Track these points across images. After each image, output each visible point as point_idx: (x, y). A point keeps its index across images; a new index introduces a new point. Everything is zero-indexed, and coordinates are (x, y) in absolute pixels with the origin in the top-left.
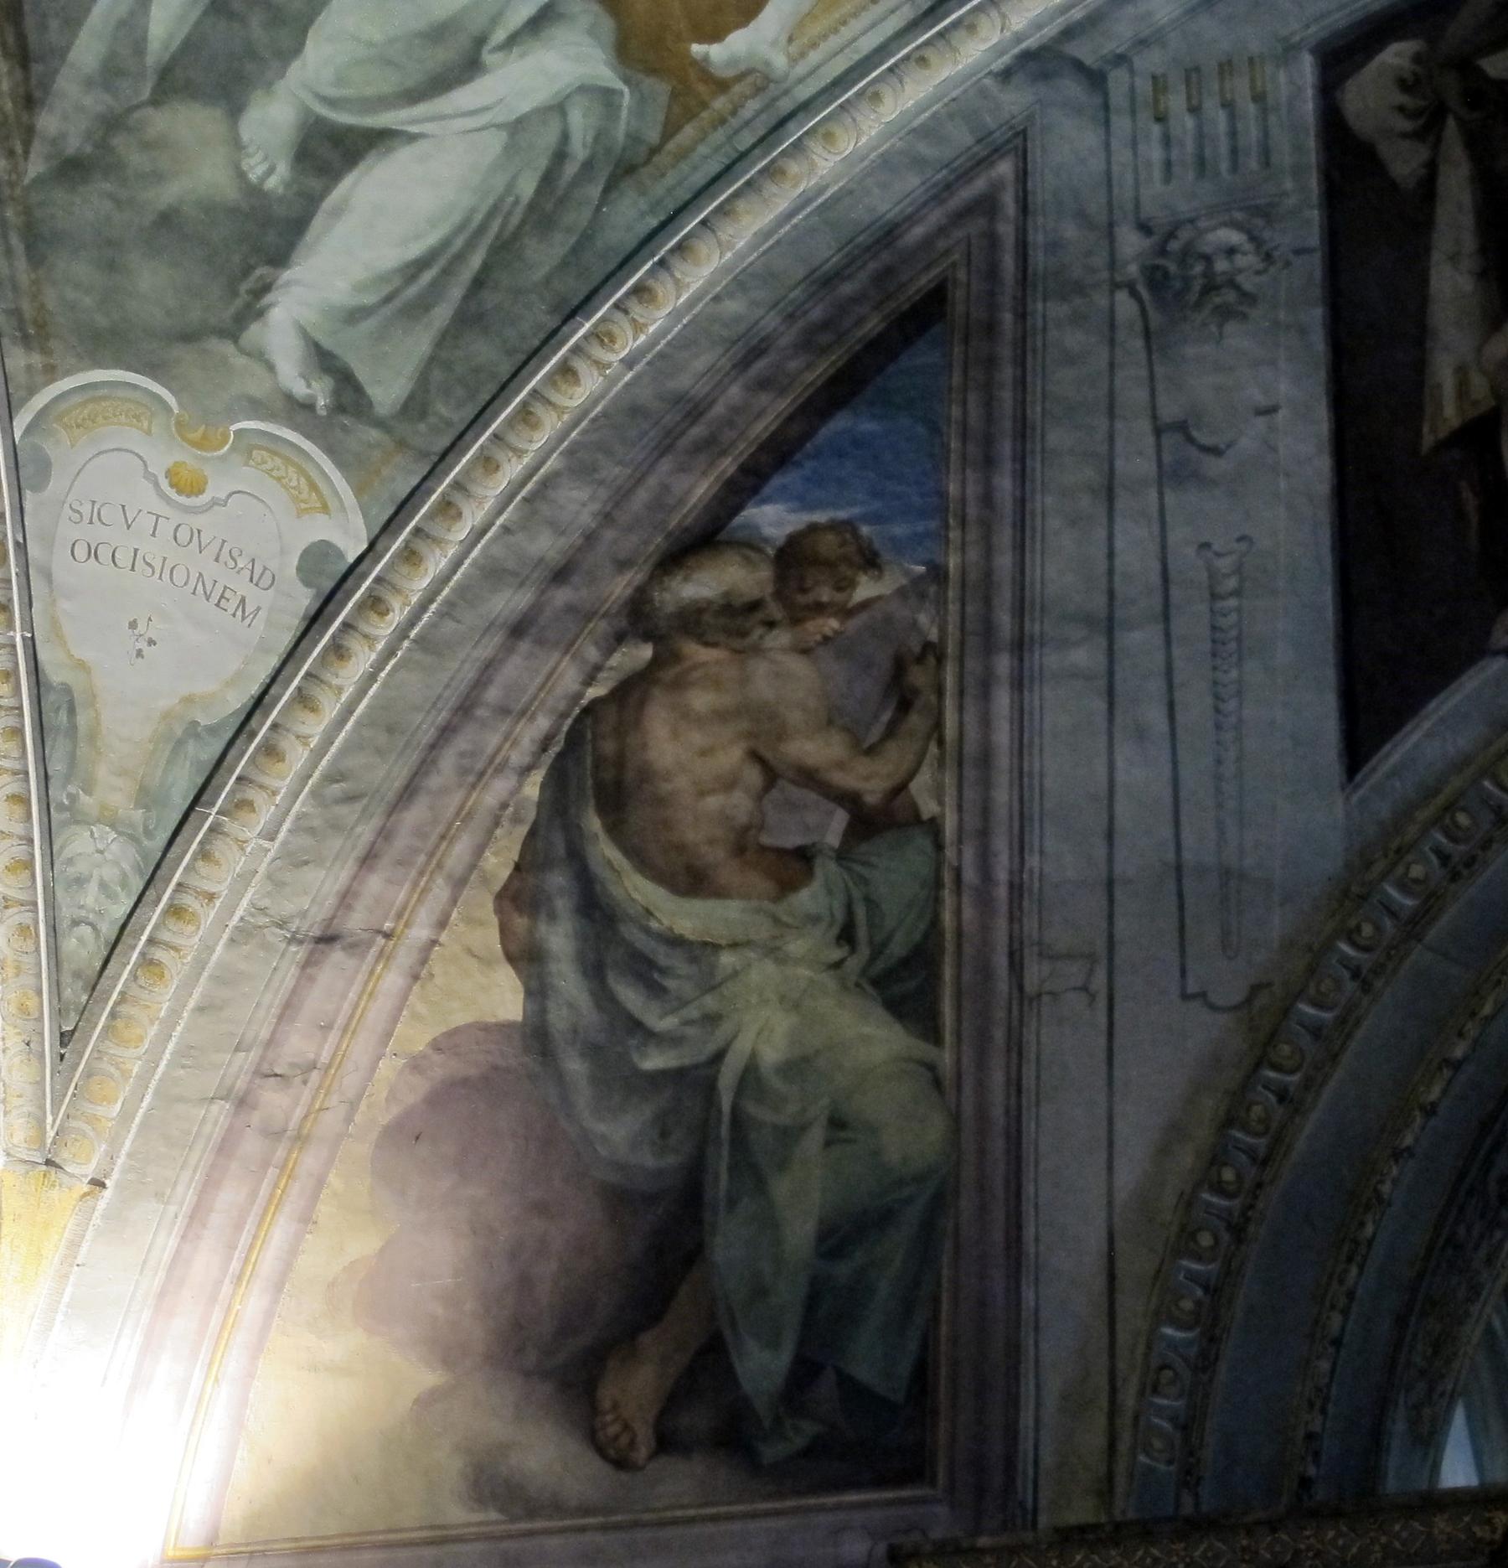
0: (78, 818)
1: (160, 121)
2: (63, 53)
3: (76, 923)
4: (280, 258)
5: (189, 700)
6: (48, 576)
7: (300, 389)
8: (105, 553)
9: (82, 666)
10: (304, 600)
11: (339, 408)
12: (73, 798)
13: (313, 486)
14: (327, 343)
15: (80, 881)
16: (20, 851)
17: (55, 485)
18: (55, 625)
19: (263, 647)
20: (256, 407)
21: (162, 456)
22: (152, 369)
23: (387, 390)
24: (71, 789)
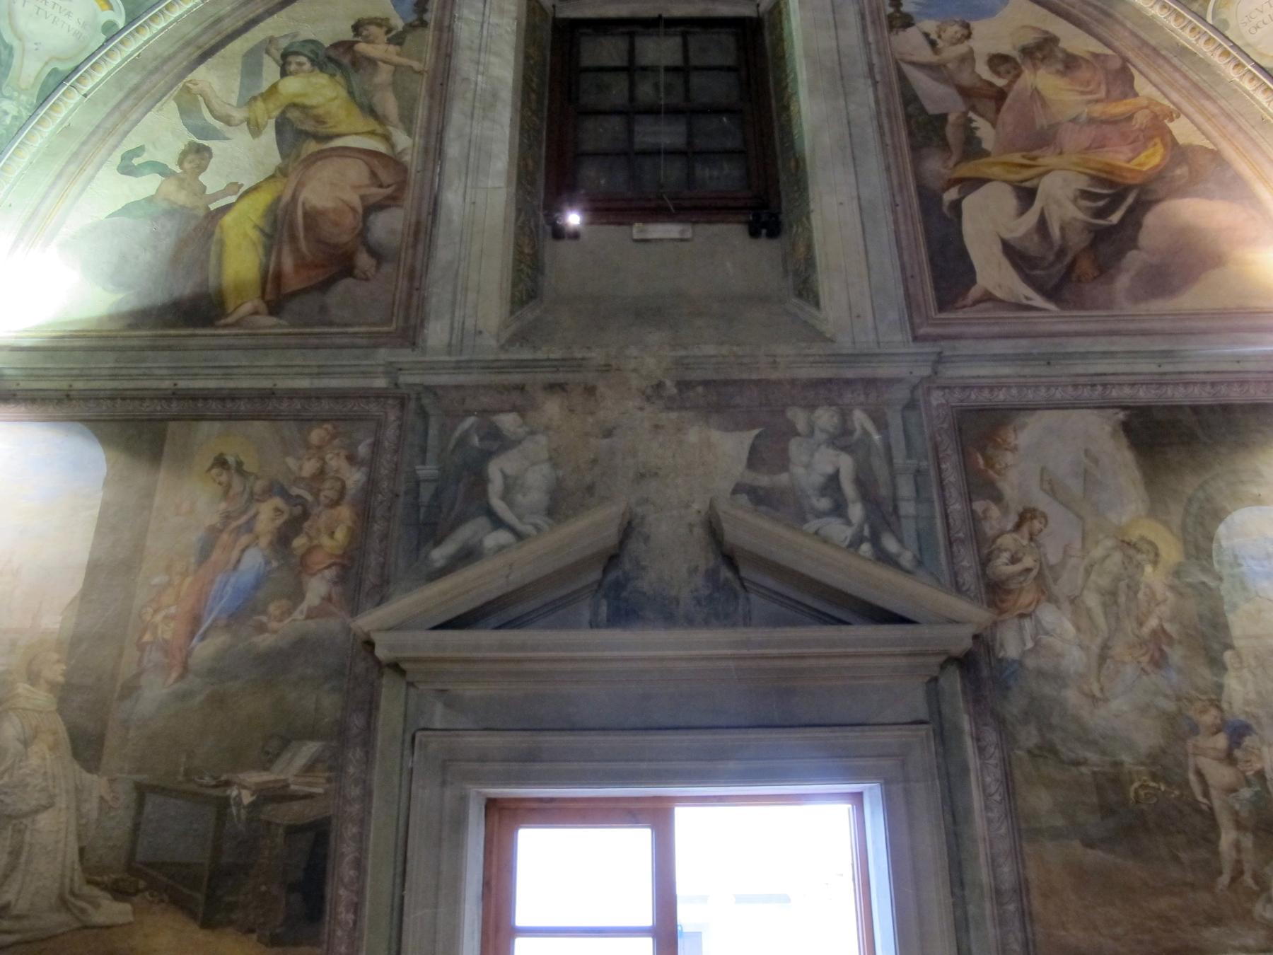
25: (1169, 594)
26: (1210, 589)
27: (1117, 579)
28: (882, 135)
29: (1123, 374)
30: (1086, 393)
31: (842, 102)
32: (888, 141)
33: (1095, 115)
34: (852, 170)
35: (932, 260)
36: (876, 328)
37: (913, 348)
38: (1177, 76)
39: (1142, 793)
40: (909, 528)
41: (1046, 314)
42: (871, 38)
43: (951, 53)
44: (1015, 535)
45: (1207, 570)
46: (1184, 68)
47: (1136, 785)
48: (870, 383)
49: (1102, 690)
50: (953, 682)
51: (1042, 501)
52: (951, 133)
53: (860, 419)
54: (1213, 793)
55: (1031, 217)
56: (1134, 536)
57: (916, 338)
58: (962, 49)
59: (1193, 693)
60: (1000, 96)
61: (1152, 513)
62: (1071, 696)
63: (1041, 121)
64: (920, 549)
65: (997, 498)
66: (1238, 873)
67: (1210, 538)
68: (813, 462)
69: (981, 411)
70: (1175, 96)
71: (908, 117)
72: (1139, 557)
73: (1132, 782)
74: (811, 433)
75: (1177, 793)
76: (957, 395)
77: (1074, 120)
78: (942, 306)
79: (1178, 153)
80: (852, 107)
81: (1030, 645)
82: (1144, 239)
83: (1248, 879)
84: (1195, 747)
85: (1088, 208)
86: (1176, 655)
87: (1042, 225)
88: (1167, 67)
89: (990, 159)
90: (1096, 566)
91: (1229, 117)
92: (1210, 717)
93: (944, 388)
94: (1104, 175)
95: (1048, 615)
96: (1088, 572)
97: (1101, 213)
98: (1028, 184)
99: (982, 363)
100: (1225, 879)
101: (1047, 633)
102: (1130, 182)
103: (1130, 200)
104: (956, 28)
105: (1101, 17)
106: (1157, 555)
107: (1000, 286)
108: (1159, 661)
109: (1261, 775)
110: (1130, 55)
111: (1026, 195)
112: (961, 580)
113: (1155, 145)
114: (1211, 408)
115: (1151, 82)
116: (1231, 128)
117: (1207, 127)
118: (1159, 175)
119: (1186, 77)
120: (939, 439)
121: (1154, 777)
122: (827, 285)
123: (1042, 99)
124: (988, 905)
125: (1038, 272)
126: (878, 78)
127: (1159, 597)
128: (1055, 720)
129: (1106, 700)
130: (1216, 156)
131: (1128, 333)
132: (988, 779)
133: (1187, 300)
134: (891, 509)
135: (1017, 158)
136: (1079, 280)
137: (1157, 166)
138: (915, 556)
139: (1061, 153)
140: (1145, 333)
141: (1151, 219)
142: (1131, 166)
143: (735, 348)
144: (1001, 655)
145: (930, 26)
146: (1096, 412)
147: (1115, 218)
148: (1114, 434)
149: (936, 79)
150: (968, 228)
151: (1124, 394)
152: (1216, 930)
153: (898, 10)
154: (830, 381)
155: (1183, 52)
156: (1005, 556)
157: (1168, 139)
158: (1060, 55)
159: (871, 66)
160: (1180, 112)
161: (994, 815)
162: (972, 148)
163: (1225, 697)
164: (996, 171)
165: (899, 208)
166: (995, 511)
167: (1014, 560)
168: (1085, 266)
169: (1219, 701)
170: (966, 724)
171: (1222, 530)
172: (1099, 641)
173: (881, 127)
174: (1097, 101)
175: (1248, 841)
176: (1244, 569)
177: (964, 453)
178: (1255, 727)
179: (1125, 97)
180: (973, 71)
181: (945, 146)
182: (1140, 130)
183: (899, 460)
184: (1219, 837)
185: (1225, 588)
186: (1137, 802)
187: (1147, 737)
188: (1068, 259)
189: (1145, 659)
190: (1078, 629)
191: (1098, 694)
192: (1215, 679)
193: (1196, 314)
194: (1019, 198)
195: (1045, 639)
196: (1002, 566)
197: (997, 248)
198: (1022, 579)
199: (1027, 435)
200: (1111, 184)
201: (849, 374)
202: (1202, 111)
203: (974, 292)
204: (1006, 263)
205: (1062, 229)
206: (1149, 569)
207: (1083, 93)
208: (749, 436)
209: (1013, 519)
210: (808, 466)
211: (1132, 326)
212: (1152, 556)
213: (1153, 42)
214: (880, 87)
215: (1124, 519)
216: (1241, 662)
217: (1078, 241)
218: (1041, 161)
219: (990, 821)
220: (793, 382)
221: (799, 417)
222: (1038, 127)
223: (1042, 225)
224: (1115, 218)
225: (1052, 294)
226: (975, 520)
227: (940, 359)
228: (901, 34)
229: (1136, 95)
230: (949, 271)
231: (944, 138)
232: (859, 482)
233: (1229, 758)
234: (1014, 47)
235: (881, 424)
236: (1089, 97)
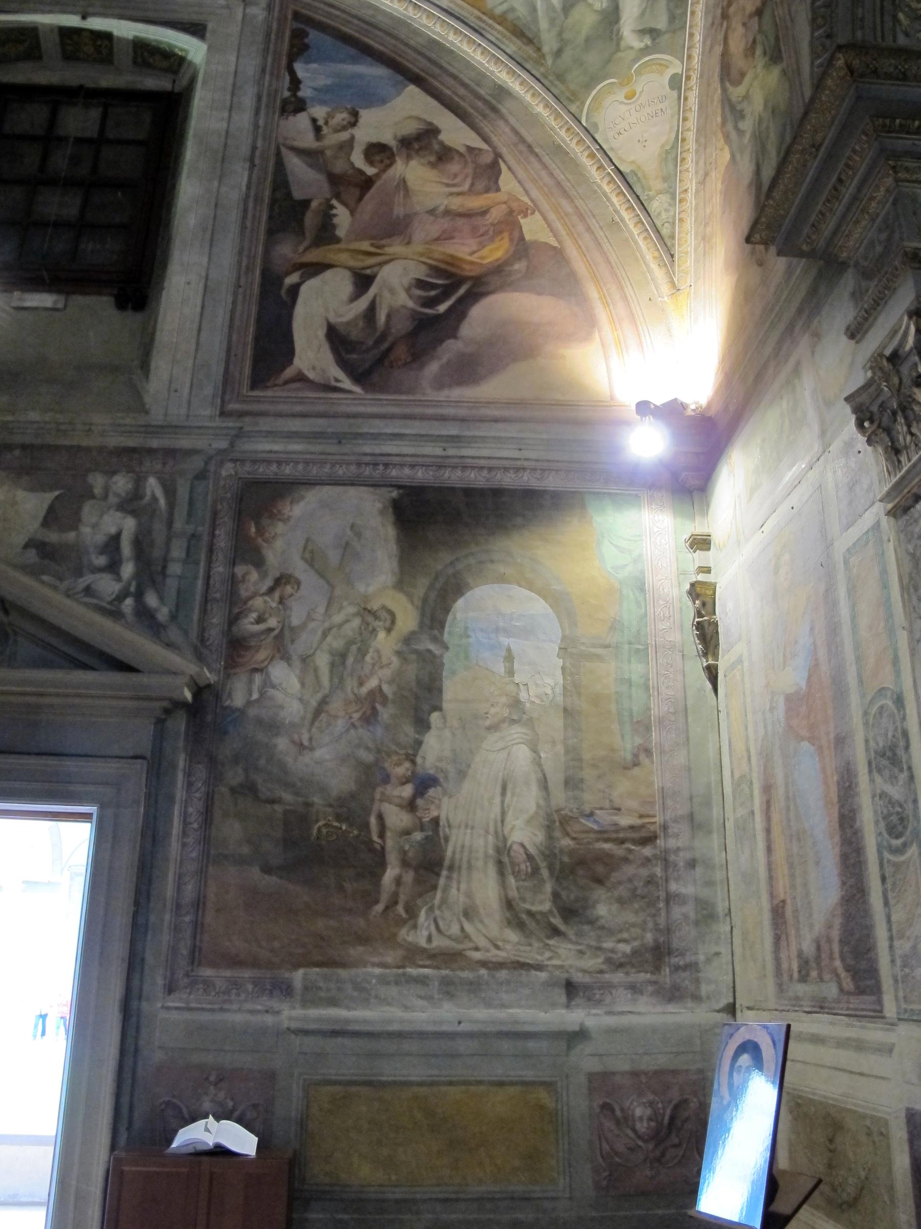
0: (651, 199)
1: (571, 20)
2: (539, 30)
4: (617, 20)
5: (663, 146)
6: (612, 149)
7: (642, 45)
8: (622, 131)
9: (633, 162)
10: (675, 94)
11: (654, 39)
12: (648, 195)
13: (660, 65)
14: (640, 28)
15: (659, 214)
16: (636, 219)
17: (601, 127)
18: (620, 159)
19: (672, 116)
20: (635, 60)
21: (620, 96)
22: (605, 79)
23: (661, 23)
25: (395, 660)
26: (434, 656)
27: (350, 643)
28: (244, 217)
30: (368, 471)
31: (216, 183)
32: (249, 224)
33: (453, 207)
34: (207, 250)
36: (189, 403)
37: (218, 422)
38: (544, 173)
39: (324, 831)
40: (172, 585)
41: (351, 396)
42: (261, 123)
43: (332, 139)
44: (267, 598)
45: (436, 640)
46: (553, 166)
47: (321, 823)
48: (170, 453)
49: (310, 739)
50: (179, 724)
51: (299, 569)
52: (310, 220)
53: (153, 485)
54: (388, 834)
55: (363, 304)
56: (375, 605)
57: (223, 414)
58: (344, 136)
59: (394, 747)
60: (367, 183)
61: (400, 585)
62: (282, 744)
63: (399, 211)
64: (177, 606)
65: (259, 562)
66: (393, 902)
67: (447, 610)
68: (104, 522)
69: (266, 483)
70: (535, 193)
71: (273, 202)
72: (377, 624)
73: (317, 821)
74: (105, 497)
75: (356, 832)
76: (248, 467)
77: (432, 212)
79: (522, 248)
80: (224, 189)
81: (255, 696)
83: (400, 909)
84: (383, 794)
85: (420, 297)
86: (385, 714)
87: (371, 312)
88: (537, 166)
90: (335, 630)
91: (582, 217)
92: (402, 770)
93: (234, 461)
94: (443, 266)
95: (279, 672)
96: (325, 635)
98: (368, 272)
100: (379, 907)
101: (274, 687)
103: (462, 291)
104: (345, 115)
105: (487, 111)
106: (393, 622)
107: (314, 368)
108: (370, 718)
109: (436, 821)
110: (504, 151)
112: (206, 635)
113: (503, 239)
114: (481, 492)
115: (516, 177)
116: (581, 228)
117: (558, 225)
118: (499, 269)
119: (551, 174)
120: (219, 507)
121: (338, 817)
123: (406, 189)
124: (167, 917)
125: (354, 356)
126: (257, 161)
127: (385, 661)
128: (262, 762)
129: (312, 749)
130: (558, 253)
131: (423, 418)
132: (190, 810)
134: (159, 568)
135: (365, 246)
137: (497, 260)
138: (170, 612)
139: (408, 243)
141: (477, 311)
143: (58, 416)
144: (227, 703)
145: (319, 112)
146: (371, 489)
147: (442, 308)
148: (382, 512)
149: (310, 166)
150: (300, 310)
151: (405, 475)
152: (361, 949)
153: (294, 95)
154: (133, 450)
155: (558, 150)
156: (254, 615)
158: (436, 147)
159: (254, 148)
160: (537, 208)
161: (190, 840)
162: (326, 233)
163: (421, 753)
164: (344, 258)
165: (241, 290)
166: (254, 576)
167: (260, 620)
168: (401, 352)
169: (415, 755)
170: (181, 761)
171: (460, 603)
172: (319, 696)
173: (245, 211)
174: (458, 194)
175: (409, 877)
176: (471, 640)
178: (441, 780)
179: (487, 190)
180: (349, 159)
182: (492, 224)
183: (178, 525)
184: (384, 871)
185: (448, 658)
186: (318, 838)
187: (341, 781)
188: (386, 345)
189: (356, 716)
190: (303, 684)
191: (306, 743)
192: (417, 736)
195: (271, 692)
196: (248, 625)
197: (321, 333)
198: (263, 637)
199: (299, 508)
201: (154, 443)
203: (289, 372)
205: (389, 316)
206: (382, 635)
207: (448, 185)
208: (50, 496)
209: (269, 582)
210: (95, 526)
212: (388, 624)
213: (529, 139)
214: (256, 169)
215: (371, 589)
216: (445, 722)
217: (402, 326)
218: (388, 250)
219: (184, 845)
220: (101, 449)
221: (97, 481)
222: (394, 217)
224: (442, 308)
225: (359, 377)
226: (233, 582)
227: (240, 434)
228: (291, 118)
229: (498, 190)
232: (138, 543)
233: (411, 806)
234: (395, 138)
235: (170, 492)
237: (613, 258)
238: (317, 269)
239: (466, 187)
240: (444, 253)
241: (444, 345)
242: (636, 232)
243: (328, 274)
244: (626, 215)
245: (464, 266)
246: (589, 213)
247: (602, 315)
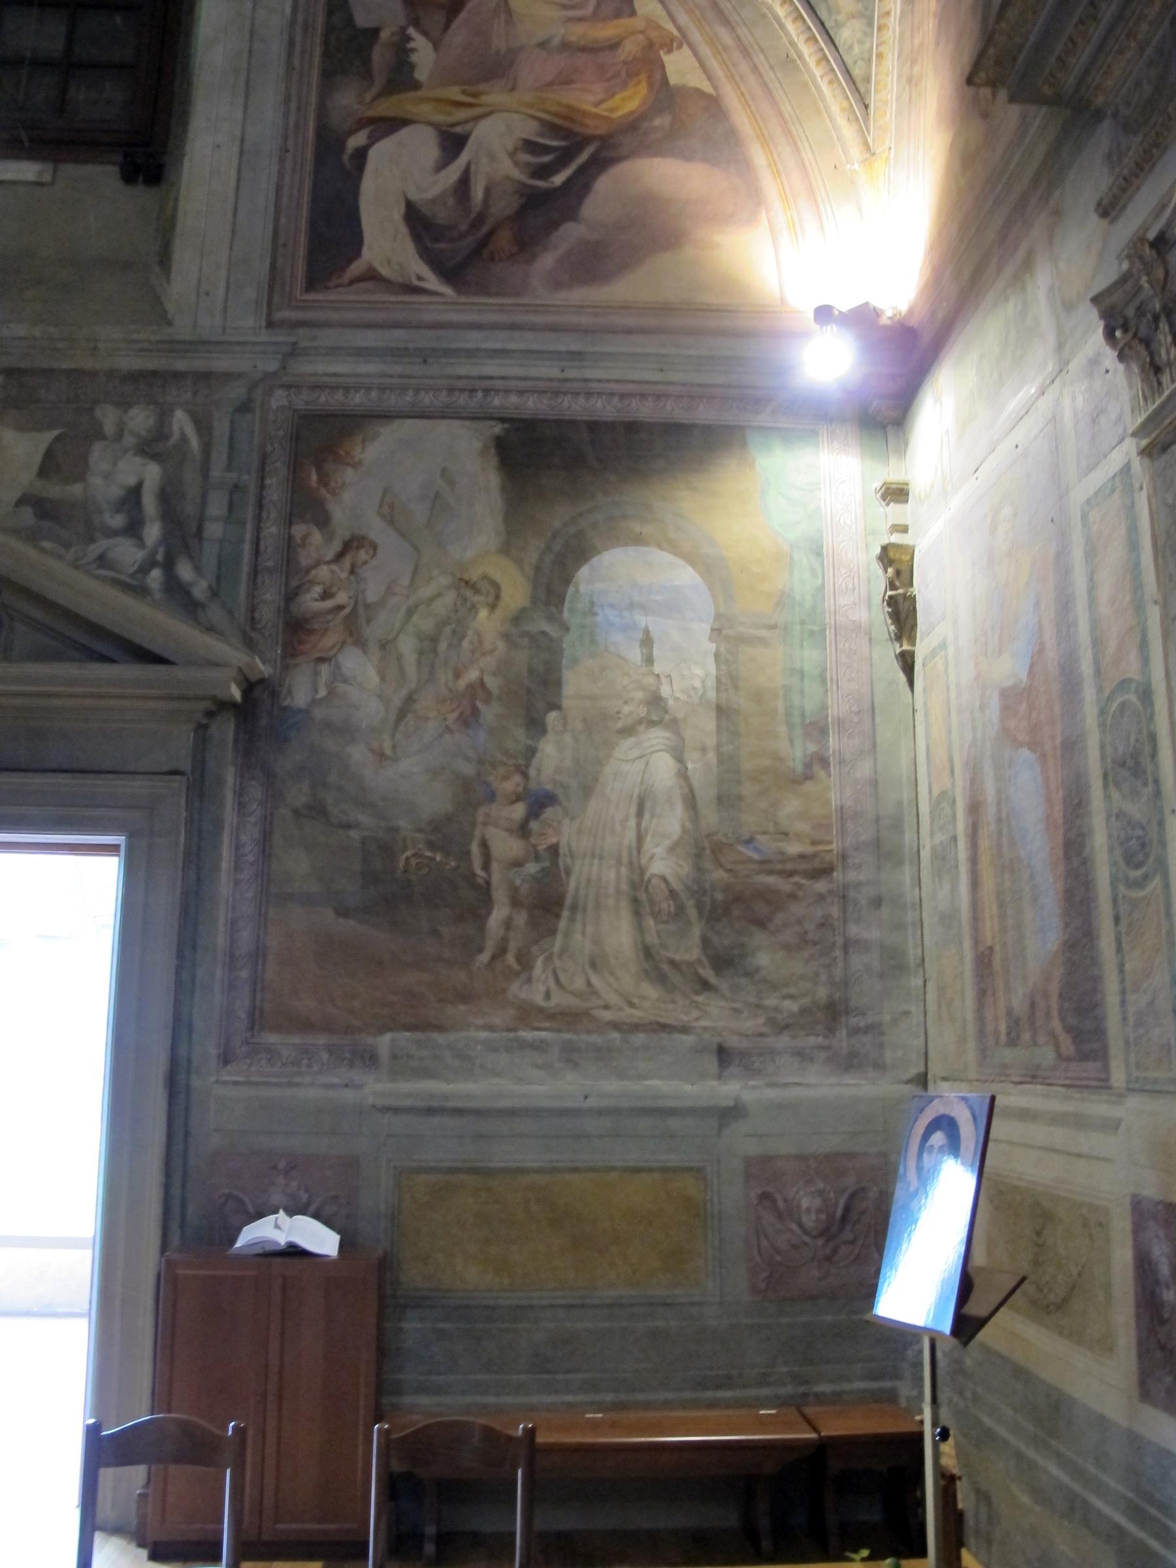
0: (839, 25)
3: (855, 63)
12: (836, 21)
15: (851, 47)
24: (833, 18)
25: (501, 645)
26: (551, 640)
27: (442, 623)
28: (290, 54)
29: (514, 378)
30: (462, 399)
32: (296, 62)
33: (573, 39)
35: (312, 225)
36: (225, 310)
37: (264, 336)
39: (414, 862)
40: (210, 553)
41: (439, 299)
44: (334, 567)
45: (551, 618)
47: (408, 853)
48: (206, 377)
49: (394, 747)
50: (225, 730)
51: (377, 529)
52: (379, 56)
53: (181, 421)
54: (495, 866)
55: (453, 173)
56: (474, 575)
59: (499, 756)
61: (505, 549)
62: (358, 753)
63: (499, 44)
64: (218, 579)
65: (323, 521)
66: (502, 950)
67: (567, 580)
68: (116, 471)
69: (327, 417)
70: (683, 19)
72: (476, 599)
73: (405, 849)
74: (119, 436)
75: (453, 864)
76: (305, 395)
77: (542, 45)
78: (312, 284)
79: (666, 97)
81: (322, 693)
82: (589, 209)
83: (510, 958)
84: (487, 815)
85: (528, 164)
86: (489, 713)
87: (464, 183)
89: (419, 93)
90: (422, 607)
91: (746, 52)
92: (512, 784)
93: (288, 387)
94: (560, 122)
95: (351, 660)
96: (410, 612)
97: (542, 172)
98: (458, 129)
99: (344, 358)
100: (485, 957)
101: (345, 681)
102: (590, 132)
106: (498, 597)
107: (389, 262)
108: (469, 719)
109: (554, 850)
111: (453, 143)
112: (257, 615)
113: (639, 83)
114: (611, 426)
116: (744, 67)
117: (713, 63)
118: (633, 125)
120: (269, 448)
121: (431, 845)
122: (184, 256)
124: (219, 973)
125: (442, 245)
127: (487, 645)
128: (332, 778)
129: (396, 759)
130: (713, 104)
131: (533, 328)
132: (244, 838)
133: (620, 290)
134: (194, 529)
135: (455, 93)
136: (492, 259)
137: (632, 112)
138: (210, 587)
139: (512, 89)
140: (554, 329)
141: (604, 184)
142: (601, 110)
143: (52, 330)
144: (286, 703)
146: (467, 423)
147: (558, 179)
148: (483, 453)
150: (369, 185)
151: (512, 404)
152: (462, 1008)
154: (154, 373)
156: (318, 589)
157: (658, 76)
161: (245, 875)
162: (401, 77)
163: (535, 762)
164: (425, 110)
166: (317, 537)
167: (326, 595)
168: (504, 240)
169: (528, 766)
170: (230, 776)
171: (584, 572)
172: (404, 692)
173: (291, 43)
174: (580, 20)
175: (521, 919)
176: (599, 619)
177: (296, 467)
178: (561, 797)
179: (618, 15)
181: (367, 75)
182: (625, 63)
183: (216, 473)
184: (489, 913)
185: (568, 640)
186: (405, 871)
187: (434, 800)
188: (485, 229)
189: (452, 717)
190: (383, 678)
191: (388, 751)
192: (530, 742)
193: (625, 308)
194: (443, 148)
195: (341, 687)
196: (310, 601)
197: (398, 213)
198: (330, 617)
199: (375, 448)
200: (567, 134)
201: (181, 365)
202: (713, 41)
203: (356, 268)
204: (404, 230)
205: (488, 192)
206: (483, 613)
208: (50, 435)
209: (337, 546)
210: (108, 476)
211: (538, 319)
212: (491, 599)
215: (470, 554)
216: (565, 724)
217: (504, 206)
218: (486, 99)
219: (237, 883)
220: (111, 374)
221: (108, 417)
223: (464, 183)
224: (558, 179)
225: (452, 273)
226: (290, 546)
227: (294, 352)
229: (633, 13)
230: (331, 236)
231: (367, 61)
232: (166, 498)
233: (523, 830)
235: (203, 426)
236: (571, 13)
237: (787, 109)
238: (392, 124)
239: (589, 10)
240: (560, 104)
241: (562, 228)
242: (818, 72)
243: (404, 133)
244: (806, 50)
245: (587, 121)
246: (756, 47)
247: (769, 185)
